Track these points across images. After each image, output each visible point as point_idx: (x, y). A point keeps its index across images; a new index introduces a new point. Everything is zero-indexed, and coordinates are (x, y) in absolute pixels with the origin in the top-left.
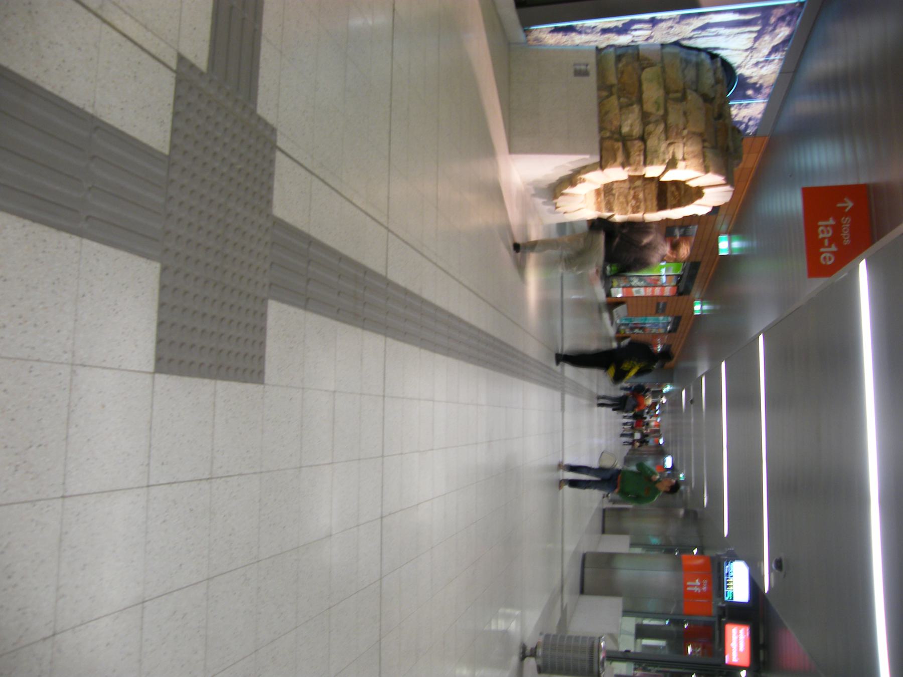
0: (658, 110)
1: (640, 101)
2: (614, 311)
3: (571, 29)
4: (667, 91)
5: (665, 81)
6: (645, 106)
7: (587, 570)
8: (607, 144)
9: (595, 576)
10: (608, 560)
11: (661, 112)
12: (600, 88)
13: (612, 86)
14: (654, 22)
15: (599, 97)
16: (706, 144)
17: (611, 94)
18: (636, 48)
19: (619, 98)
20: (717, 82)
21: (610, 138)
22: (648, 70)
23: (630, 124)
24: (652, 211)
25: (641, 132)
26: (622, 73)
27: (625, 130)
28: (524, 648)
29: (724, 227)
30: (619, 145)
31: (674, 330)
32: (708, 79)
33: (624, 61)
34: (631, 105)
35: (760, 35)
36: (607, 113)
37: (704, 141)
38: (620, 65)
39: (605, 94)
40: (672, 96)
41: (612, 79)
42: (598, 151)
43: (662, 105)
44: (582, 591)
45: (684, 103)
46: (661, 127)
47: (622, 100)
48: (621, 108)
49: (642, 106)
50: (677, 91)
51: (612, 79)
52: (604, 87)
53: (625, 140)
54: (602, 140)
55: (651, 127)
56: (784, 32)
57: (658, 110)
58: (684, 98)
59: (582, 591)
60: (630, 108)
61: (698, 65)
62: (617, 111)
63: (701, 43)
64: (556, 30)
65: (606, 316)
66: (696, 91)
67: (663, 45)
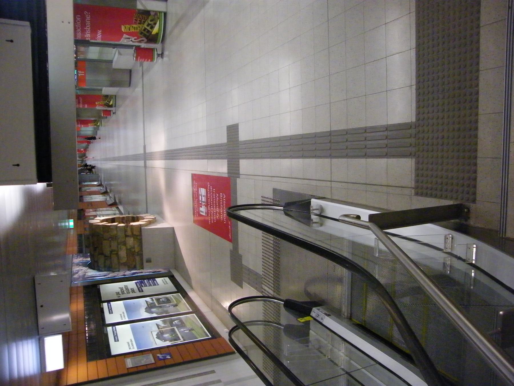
1: (127, 249)
2: (114, 201)
4: (117, 254)
7: (129, 80)
9: (125, 78)
10: (113, 84)
11: (119, 246)
12: (142, 254)
13: (137, 255)
14: (124, 275)
20: (97, 262)
21: (137, 236)
22: (124, 261)
23: (131, 241)
24: (117, 218)
27: (132, 239)
28: (162, 57)
29: (72, 232)
30: (135, 233)
31: (81, 197)
33: (133, 266)
35: (85, 275)
39: (139, 253)
40: (116, 252)
41: (138, 258)
42: (143, 231)
44: (130, 71)
46: (119, 241)
48: (134, 248)
52: (140, 254)
53: (133, 235)
54: (141, 235)
55: (123, 240)
56: (76, 276)
58: (111, 252)
59: (130, 71)
61: (105, 266)
65: (117, 201)
66: (105, 256)
67: (119, 271)
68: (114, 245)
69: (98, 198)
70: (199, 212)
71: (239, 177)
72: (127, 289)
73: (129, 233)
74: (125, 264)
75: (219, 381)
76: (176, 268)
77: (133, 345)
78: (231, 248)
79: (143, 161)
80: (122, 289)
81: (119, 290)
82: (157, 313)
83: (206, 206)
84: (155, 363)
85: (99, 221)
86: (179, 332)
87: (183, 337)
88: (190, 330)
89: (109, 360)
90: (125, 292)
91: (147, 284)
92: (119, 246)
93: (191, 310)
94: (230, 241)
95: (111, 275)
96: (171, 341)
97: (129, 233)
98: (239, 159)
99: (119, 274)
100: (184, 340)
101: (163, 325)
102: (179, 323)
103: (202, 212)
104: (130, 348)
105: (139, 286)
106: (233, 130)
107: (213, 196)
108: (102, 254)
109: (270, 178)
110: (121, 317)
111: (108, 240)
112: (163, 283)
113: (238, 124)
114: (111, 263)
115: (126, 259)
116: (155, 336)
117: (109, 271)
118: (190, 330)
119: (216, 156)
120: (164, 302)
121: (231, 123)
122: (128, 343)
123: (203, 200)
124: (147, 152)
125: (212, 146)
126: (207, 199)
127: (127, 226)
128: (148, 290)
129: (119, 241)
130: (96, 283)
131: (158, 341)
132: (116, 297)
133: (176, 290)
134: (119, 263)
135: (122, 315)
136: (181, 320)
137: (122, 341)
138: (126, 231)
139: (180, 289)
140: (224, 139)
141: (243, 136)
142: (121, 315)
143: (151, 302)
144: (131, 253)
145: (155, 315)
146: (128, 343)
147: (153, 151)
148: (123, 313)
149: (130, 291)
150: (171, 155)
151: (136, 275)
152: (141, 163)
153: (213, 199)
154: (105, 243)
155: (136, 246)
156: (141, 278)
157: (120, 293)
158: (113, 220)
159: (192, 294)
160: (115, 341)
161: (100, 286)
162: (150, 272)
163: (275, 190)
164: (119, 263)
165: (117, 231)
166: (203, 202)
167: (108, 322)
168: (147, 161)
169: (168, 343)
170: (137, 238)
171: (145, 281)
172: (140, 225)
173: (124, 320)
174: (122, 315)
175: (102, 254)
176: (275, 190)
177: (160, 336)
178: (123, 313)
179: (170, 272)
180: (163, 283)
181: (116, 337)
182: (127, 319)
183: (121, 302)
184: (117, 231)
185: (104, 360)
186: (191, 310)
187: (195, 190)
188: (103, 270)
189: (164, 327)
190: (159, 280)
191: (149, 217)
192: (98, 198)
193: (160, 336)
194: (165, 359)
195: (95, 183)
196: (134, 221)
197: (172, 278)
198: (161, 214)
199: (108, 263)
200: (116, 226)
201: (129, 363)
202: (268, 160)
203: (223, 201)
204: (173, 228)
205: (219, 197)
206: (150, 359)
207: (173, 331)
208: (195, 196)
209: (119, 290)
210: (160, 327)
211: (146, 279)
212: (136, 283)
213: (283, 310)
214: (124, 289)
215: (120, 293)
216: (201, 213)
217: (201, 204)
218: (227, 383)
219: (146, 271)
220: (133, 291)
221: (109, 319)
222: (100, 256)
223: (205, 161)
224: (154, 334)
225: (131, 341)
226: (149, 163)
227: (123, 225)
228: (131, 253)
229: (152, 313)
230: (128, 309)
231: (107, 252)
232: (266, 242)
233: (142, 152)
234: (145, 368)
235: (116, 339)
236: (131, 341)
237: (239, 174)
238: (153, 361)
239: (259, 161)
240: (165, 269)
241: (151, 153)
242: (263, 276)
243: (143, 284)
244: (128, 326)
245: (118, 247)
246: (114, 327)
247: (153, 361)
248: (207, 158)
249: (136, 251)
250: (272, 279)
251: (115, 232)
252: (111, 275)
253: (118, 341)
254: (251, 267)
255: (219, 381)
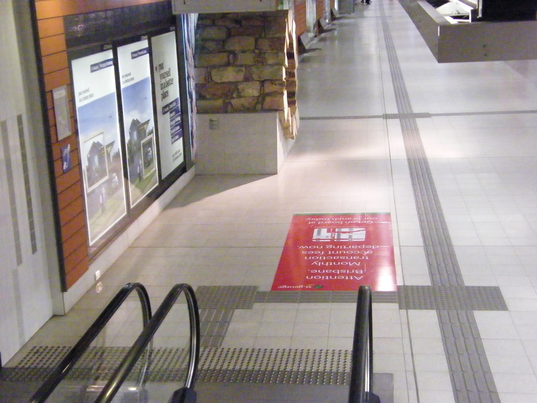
0: (242, 71)
1: (236, 83)
2: (307, 47)
3: (192, 132)
4: (228, 64)
5: (221, 66)
6: (240, 80)
8: (266, 106)
11: (243, 69)
12: (226, 112)
14: (189, 77)
15: (232, 112)
16: (263, 35)
17: (230, 103)
18: (196, 85)
19: (234, 98)
20: (214, 24)
21: (262, 104)
23: (252, 91)
25: (258, 82)
26: (214, 95)
27: (256, 93)
30: (268, 99)
32: (213, 33)
33: (203, 93)
34: (238, 89)
36: (243, 105)
37: (260, 37)
38: (208, 96)
39: (229, 108)
40: (231, 61)
41: (219, 103)
43: (238, 68)
45: (236, 52)
46: (254, 69)
47: (234, 96)
48: (239, 96)
49: (240, 82)
50: (228, 57)
51: (219, 103)
53: (263, 96)
54: (264, 110)
55: (255, 77)
57: (242, 71)
58: (233, 53)
60: (240, 90)
61: (204, 40)
62: (243, 99)
63: (193, 41)
64: (192, 144)
66: (224, 42)
67: (195, 67)
68: (247, 59)
69: (311, 17)
70: (317, 225)
71: (400, 308)
72: (169, 83)
73: (269, 88)
74: (208, 77)
75: (19, 261)
76: (197, 176)
77: (86, 98)
78: (262, 289)
79: (395, 111)
80: (168, 74)
81: (166, 70)
82: (130, 142)
83: (332, 242)
84: (57, 141)
85: (290, 29)
86: (100, 186)
87: (93, 192)
88: (102, 205)
89: (65, 55)
90: (164, 81)
91: (174, 122)
92: (243, 69)
93: (132, 207)
94: (274, 287)
95: (189, 51)
96: (89, 169)
97: (269, 88)
98: (438, 309)
99: (190, 69)
100: (88, 195)
101: (112, 154)
102: (113, 185)
103: (319, 233)
104: (80, 94)
105: (171, 106)
106: (492, 299)
107: (353, 255)
108: (229, 35)
109: (410, 368)
110: (126, 76)
111: (256, 48)
112: (174, 151)
113: (507, 310)
114: (211, 52)
115: (219, 81)
116: (96, 140)
117: (196, 47)
118: (102, 205)
119: (435, 265)
120: (146, 154)
121: (507, 294)
122: (87, 91)
123: (343, 236)
124: (419, 121)
125: (452, 255)
126: (347, 244)
127: (282, 84)
128: (167, 122)
129: (254, 69)
130: (178, 24)
131: (89, 145)
132: (155, 64)
133: (163, 177)
134: (214, 67)
135: (129, 77)
136: (117, 188)
137: (91, 81)
138: (272, 81)
139: (165, 183)
140: (471, 279)
141: (485, 320)
142: (129, 74)
143: (147, 131)
144: (230, 90)
145: (127, 138)
146: (87, 91)
147: (422, 132)
148: (132, 79)
149: (165, 90)
150: (420, 172)
151: (189, 100)
152: (393, 109)
153: (349, 256)
154: (249, 42)
155: (242, 101)
156: (184, 112)
157: (163, 71)
158: (291, 56)
159: (156, 207)
160: (92, 66)
161: (174, 33)
162: (192, 127)
163: (390, 376)
164: (214, 67)
165: (272, 65)
166: (339, 235)
167: (121, 50)
168: (397, 121)
169: (85, 164)
170: (256, 104)
171: (179, 118)
172: (283, 110)
173: (122, 80)
174: (129, 77)
175: (229, 35)
176: (390, 376)
177: (96, 148)
178: (132, 79)
179: (192, 164)
180: (174, 151)
181: (97, 67)
182: (123, 86)
183: (149, 75)
184: (272, 65)
185: (64, 47)
186: (132, 207)
187: (358, 220)
188: (198, 36)
189: (108, 155)
190: (179, 144)
191: (295, 126)
192: (311, 17)
193: (96, 148)
194: (62, 159)
195: (336, 6)
196: (288, 97)
197: (182, 169)
198: (299, 148)
199: (211, 45)
200: (282, 64)
201: (60, 94)
202: (445, 366)
203: (349, 275)
204: (276, 173)
205: (355, 267)
206: (64, 132)
207: (102, 174)
208: (346, 220)
209: (166, 70)
210: (109, 149)
211: (182, 119)
212: (176, 101)
213: (176, 386)
214: (168, 79)
215: (163, 71)
216: (316, 231)
217: (334, 231)
218: (15, 274)
219: (194, 119)
220: (165, 95)
221: (125, 52)
222: (225, 30)
223: (420, 242)
224: (99, 139)
225: (91, 96)
226: (395, 125)
227: (284, 76)
228: (230, 90)
229: (131, 134)
230: (137, 87)
231: (235, 45)
232: (286, 357)
233: (416, 110)
234: (51, 123)
235: (95, 68)
236: (91, 96)
237: (408, 308)
238: (60, 138)
239: (439, 347)
240: (196, 155)
241: (416, 129)
242: (219, 350)
243: (174, 113)
244: (114, 90)
245: (241, 66)
246: (111, 63)
247: (60, 138)
248: (426, 246)
249: (234, 102)
250: (218, 367)
251: (271, 61)
252: (189, 51)
253: (92, 71)
254: (231, 327)
255: (19, 261)
